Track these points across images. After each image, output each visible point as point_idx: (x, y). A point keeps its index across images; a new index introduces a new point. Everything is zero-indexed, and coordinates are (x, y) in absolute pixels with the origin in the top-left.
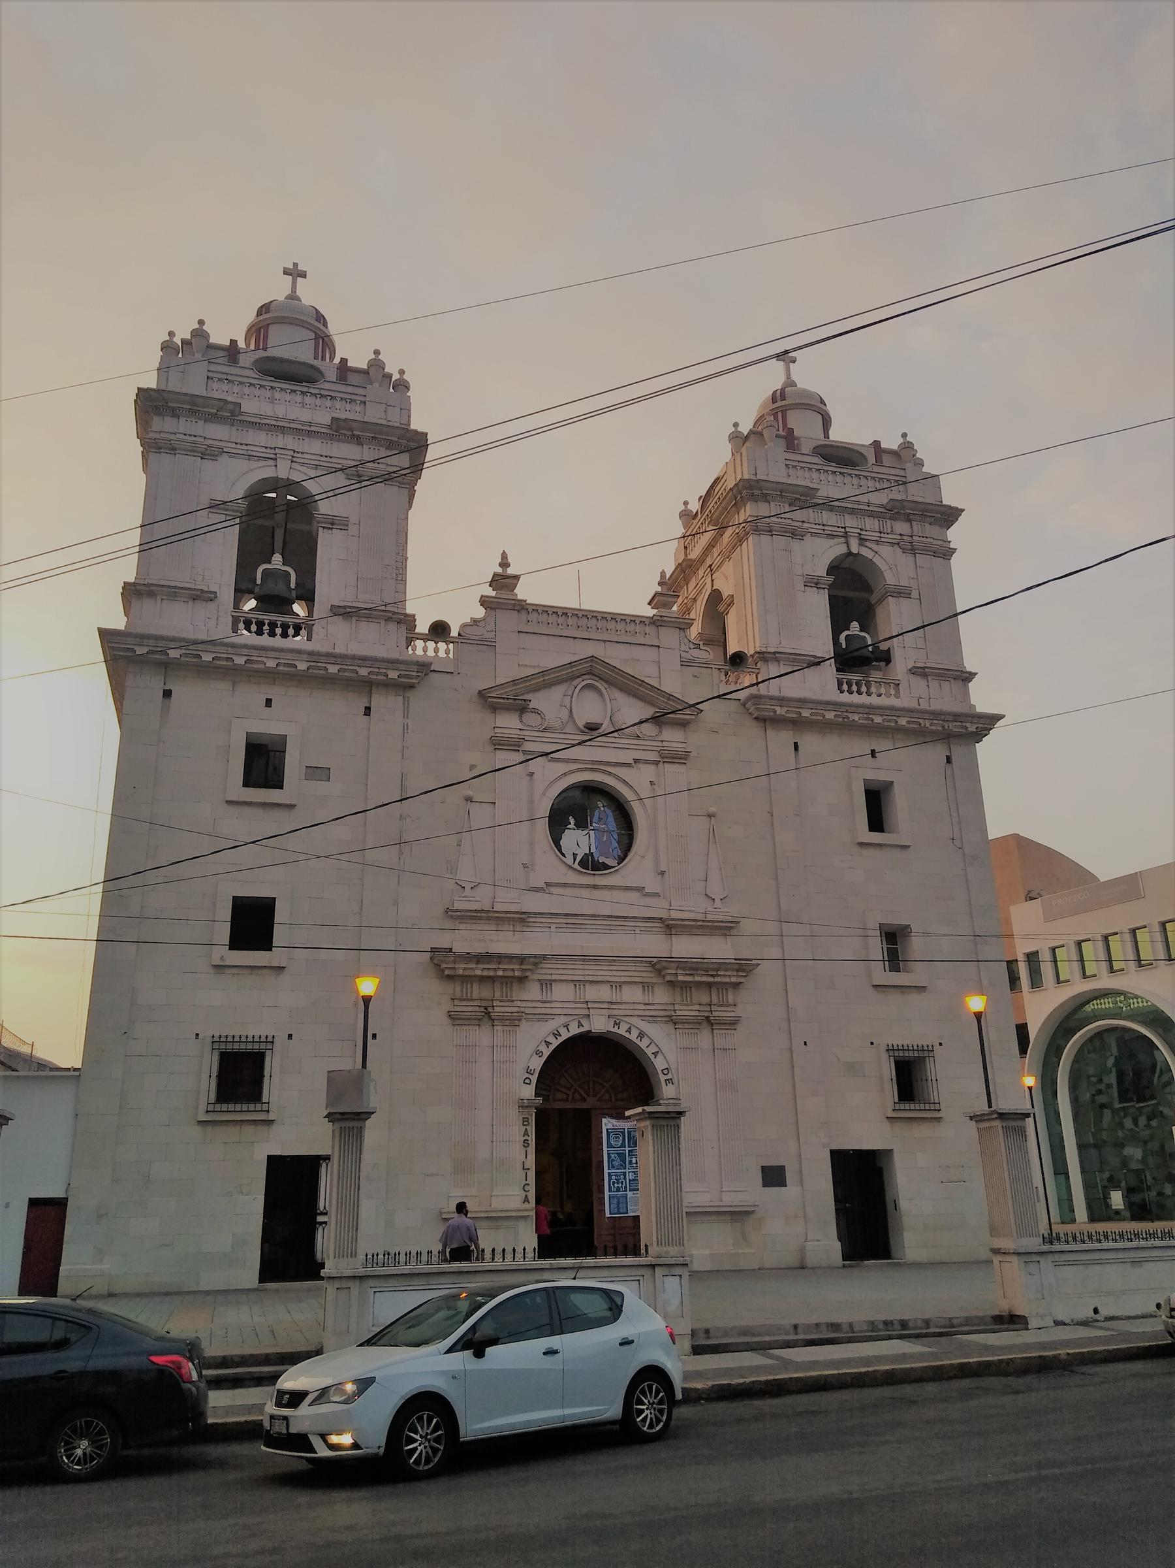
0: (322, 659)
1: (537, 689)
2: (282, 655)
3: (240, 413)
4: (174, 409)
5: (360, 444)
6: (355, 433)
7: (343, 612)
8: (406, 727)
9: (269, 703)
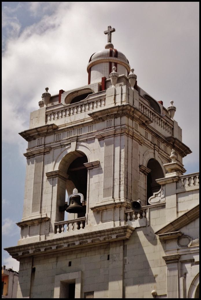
0: (84, 237)
1: (186, 224)
2: (70, 240)
3: (57, 127)
4: (33, 136)
5: (103, 121)
6: (99, 117)
7: (98, 210)
8: (124, 261)
9: (70, 264)
